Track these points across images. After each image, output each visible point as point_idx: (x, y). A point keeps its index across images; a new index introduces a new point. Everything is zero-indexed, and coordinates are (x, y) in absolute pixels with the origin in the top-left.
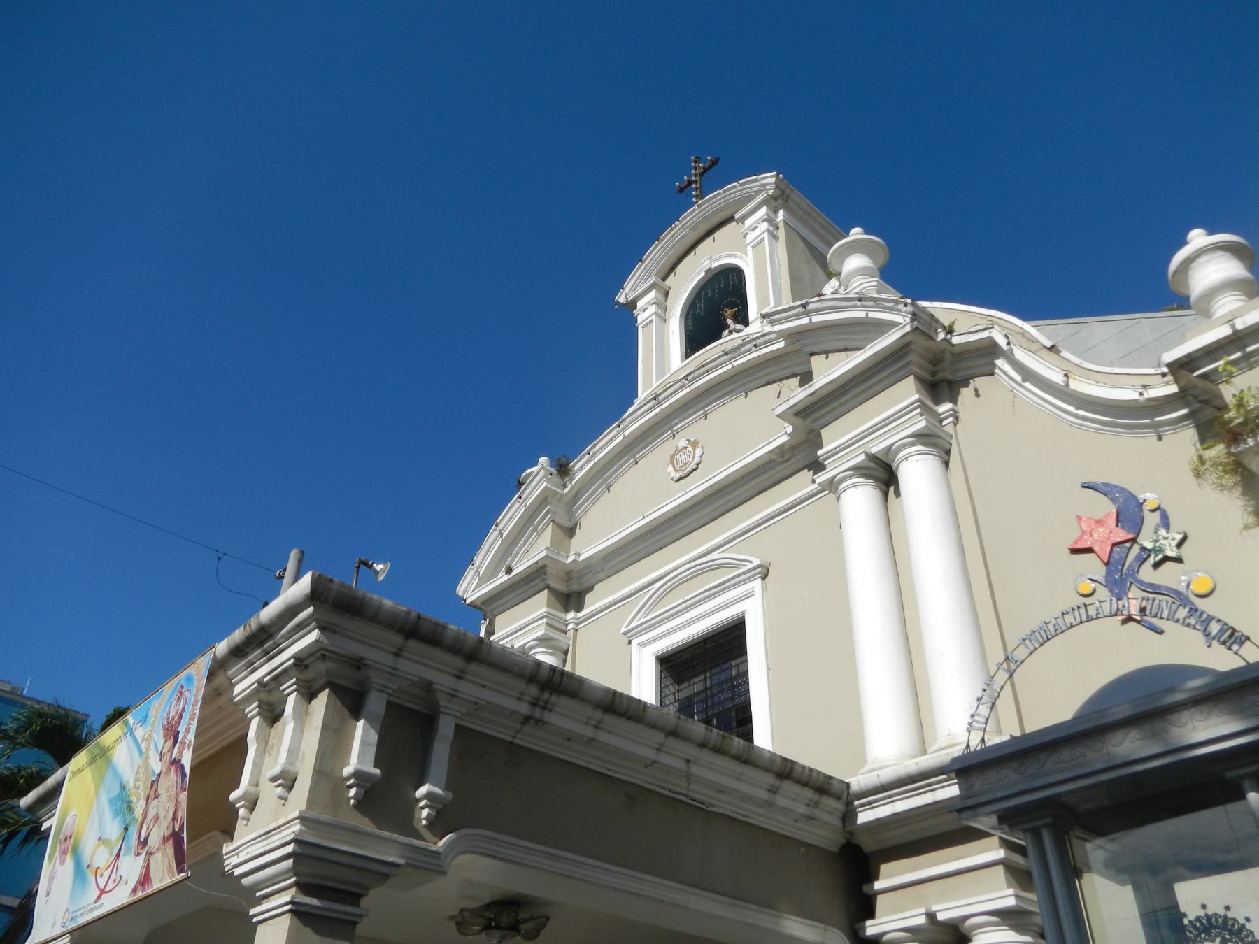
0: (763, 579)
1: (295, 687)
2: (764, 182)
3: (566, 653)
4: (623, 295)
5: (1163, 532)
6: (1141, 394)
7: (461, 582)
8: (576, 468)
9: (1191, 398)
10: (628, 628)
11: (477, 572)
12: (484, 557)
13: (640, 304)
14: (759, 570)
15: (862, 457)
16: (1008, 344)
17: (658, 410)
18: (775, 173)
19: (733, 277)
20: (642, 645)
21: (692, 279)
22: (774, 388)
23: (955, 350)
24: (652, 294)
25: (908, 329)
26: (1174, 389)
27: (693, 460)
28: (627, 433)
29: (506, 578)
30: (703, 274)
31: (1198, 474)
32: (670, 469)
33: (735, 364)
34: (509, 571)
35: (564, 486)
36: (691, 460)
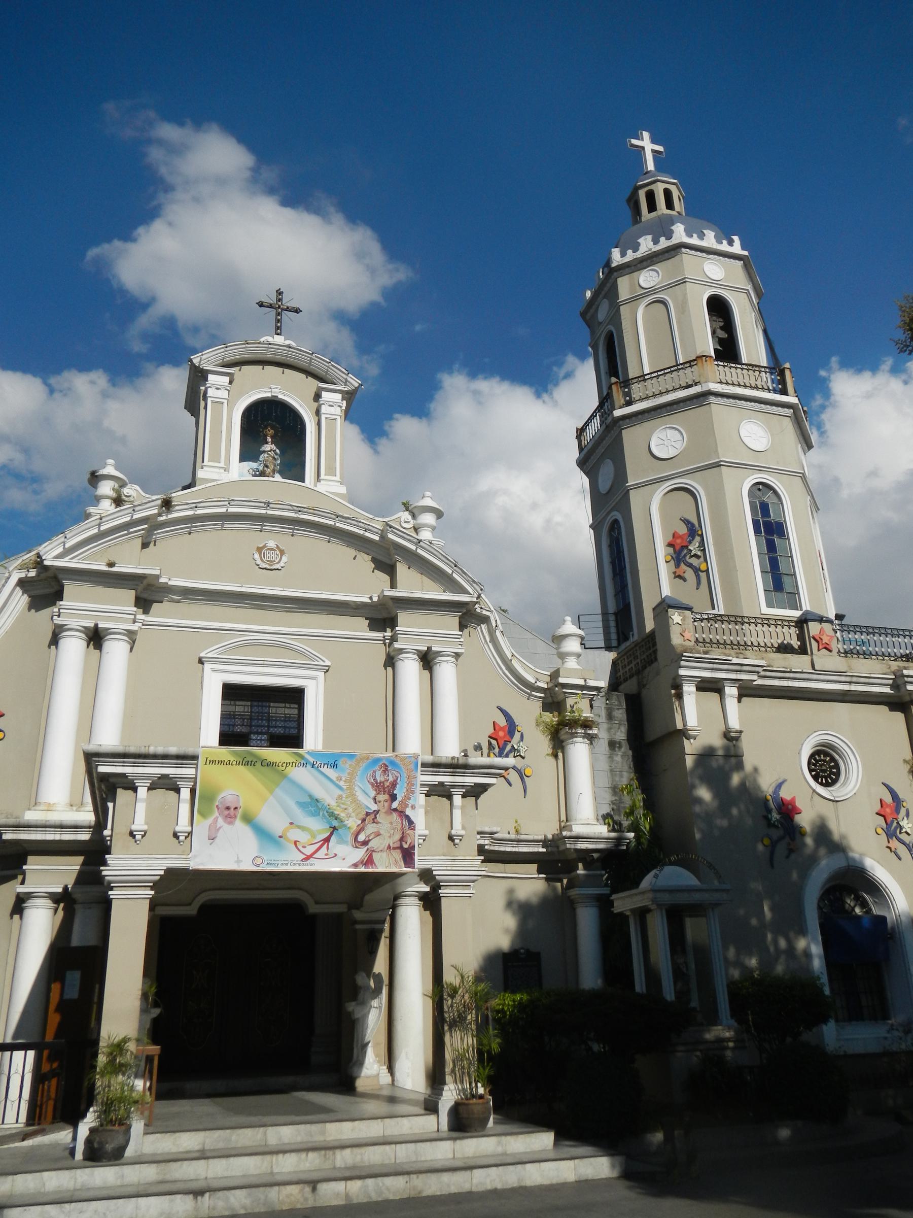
0: (325, 672)
1: (462, 793)
2: (349, 379)
3: (134, 642)
4: (199, 359)
5: (521, 744)
6: (536, 682)
7: (47, 543)
8: (177, 508)
9: (548, 692)
10: (206, 656)
11: (64, 543)
12: (76, 535)
13: (211, 378)
14: (327, 668)
15: (426, 648)
16: (496, 626)
17: (263, 512)
18: (360, 382)
19: (290, 416)
20: (214, 670)
21: (260, 392)
22: (352, 552)
23: (473, 612)
24: (227, 379)
25: (475, 600)
26: (545, 686)
27: (279, 562)
28: (232, 510)
29: (105, 568)
30: (269, 395)
31: (537, 725)
32: (257, 556)
33: (337, 525)
34: (111, 565)
35: (160, 515)
36: (278, 560)
